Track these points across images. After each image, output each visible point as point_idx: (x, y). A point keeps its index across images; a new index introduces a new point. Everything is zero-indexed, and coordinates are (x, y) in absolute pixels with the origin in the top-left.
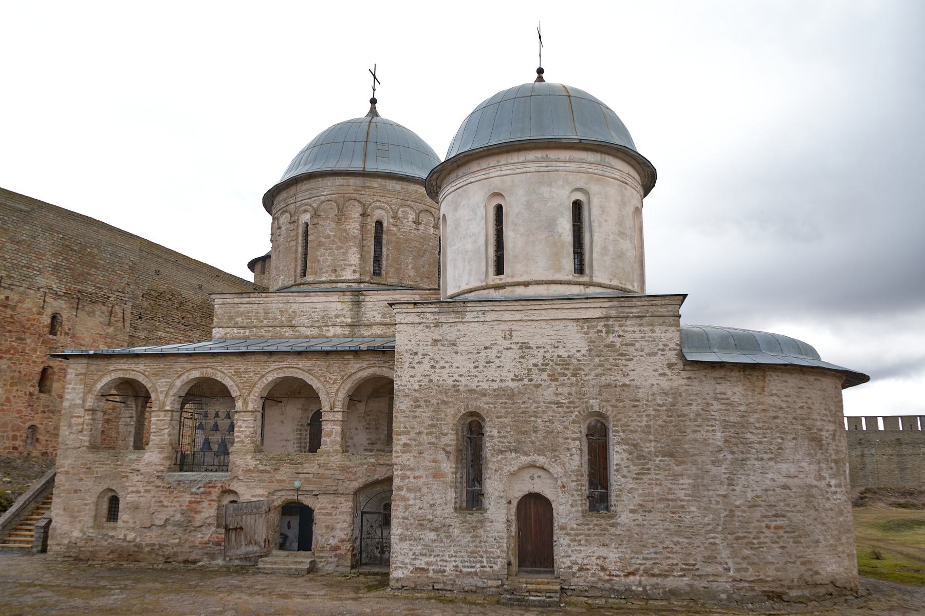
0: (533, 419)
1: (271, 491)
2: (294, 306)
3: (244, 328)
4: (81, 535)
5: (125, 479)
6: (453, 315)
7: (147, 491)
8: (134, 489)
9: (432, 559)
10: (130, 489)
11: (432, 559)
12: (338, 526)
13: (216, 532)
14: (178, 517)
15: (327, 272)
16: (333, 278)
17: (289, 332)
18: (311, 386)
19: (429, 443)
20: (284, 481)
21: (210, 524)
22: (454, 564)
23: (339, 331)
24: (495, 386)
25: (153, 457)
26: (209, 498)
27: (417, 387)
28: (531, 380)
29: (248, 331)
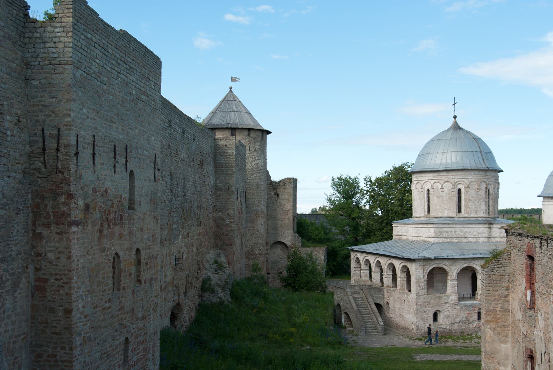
2: (466, 229)
3: (446, 238)
14: (464, 319)
16: (476, 216)
17: (464, 240)
23: (483, 239)
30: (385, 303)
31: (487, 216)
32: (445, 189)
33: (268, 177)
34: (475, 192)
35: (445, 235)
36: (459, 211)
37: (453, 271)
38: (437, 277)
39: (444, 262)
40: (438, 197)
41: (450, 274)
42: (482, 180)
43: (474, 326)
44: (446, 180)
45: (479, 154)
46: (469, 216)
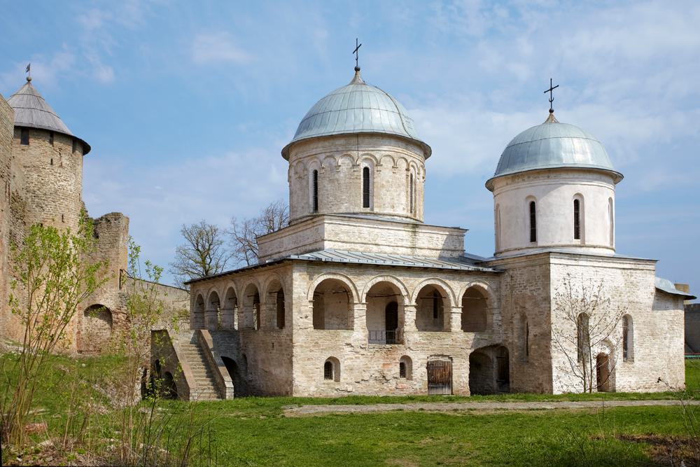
2: (377, 230)
3: (347, 242)
6: (574, 261)
7: (359, 358)
10: (346, 357)
14: (377, 375)
16: (391, 212)
17: (375, 248)
25: (359, 333)
29: (348, 245)
30: (241, 356)
31: (409, 215)
38: (331, 305)
39: (344, 271)
40: (331, 181)
42: (402, 155)
46: (381, 212)
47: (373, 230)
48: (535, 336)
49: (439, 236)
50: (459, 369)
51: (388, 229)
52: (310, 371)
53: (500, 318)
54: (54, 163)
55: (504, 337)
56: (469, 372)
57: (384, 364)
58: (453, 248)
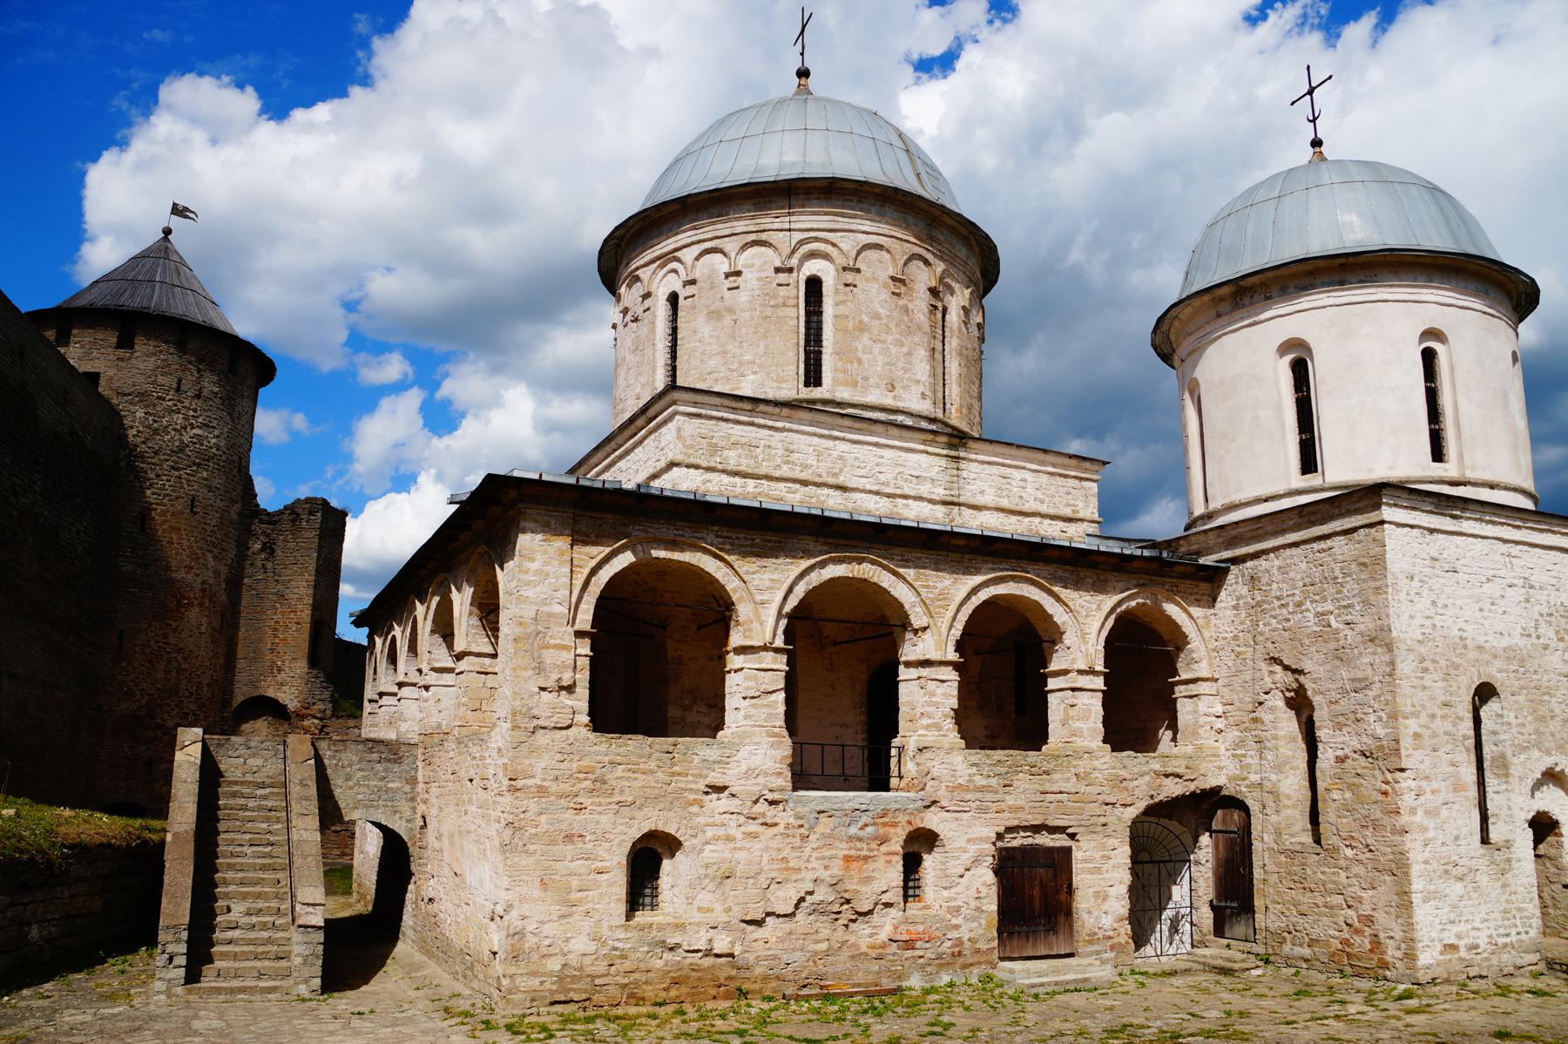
0: (1546, 698)
1: (1002, 829)
2: (843, 446)
3: (745, 475)
4: (592, 947)
5: (695, 809)
7: (753, 836)
8: (721, 832)
9: (1462, 928)
10: (710, 832)
11: (1462, 928)
12: (1112, 891)
13: (906, 921)
15: (878, 386)
16: (888, 401)
18: (1051, 616)
19: (1446, 733)
20: (1022, 808)
21: (888, 905)
22: (1489, 932)
24: (1505, 642)
26: (884, 848)
27: (1420, 637)
28: (1538, 637)
29: (751, 482)
32: (747, 274)
33: (249, 492)
34: (886, 295)
35: (733, 459)
36: (813, 376)
37: (763, 593)
40: (715, 315)
41: (743, 610)
43: (883, 936)
44: (753, 237)
45: (902, 156)
47: (830, 443)
48: (1341, 760)
49: (1029, 476)
50: (1098, 870)
51: (876, 445)
52: (575, 883)
53: (1219, 709)
54: (184, 388)
55: (1232, 768)
56: (1126, 878)
57: (848, 859)
58: (1067, 512)
